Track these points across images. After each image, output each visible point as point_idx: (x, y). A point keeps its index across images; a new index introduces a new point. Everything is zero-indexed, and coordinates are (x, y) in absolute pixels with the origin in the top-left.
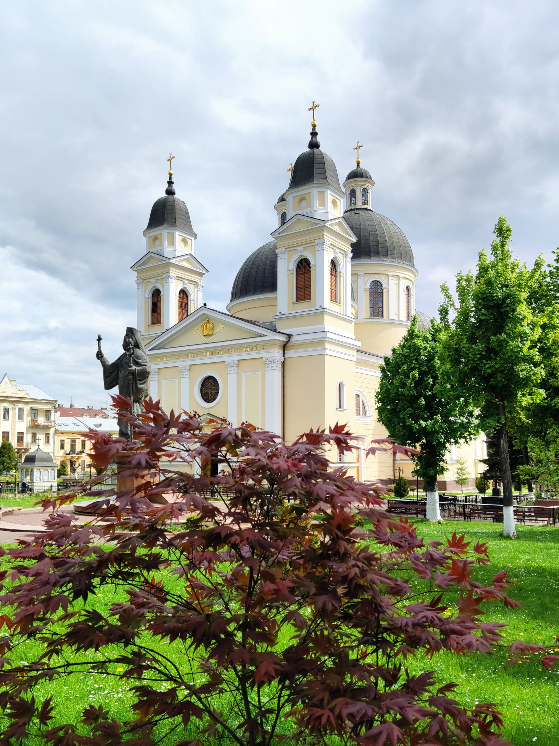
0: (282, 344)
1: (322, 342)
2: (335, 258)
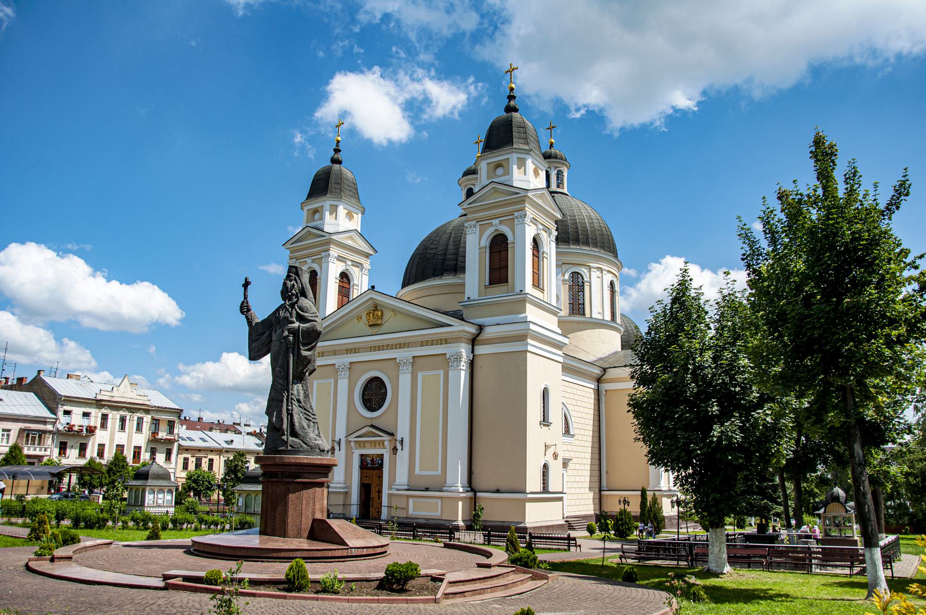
0: (471, 337)
1: (522, 338)
2: (538, 234)
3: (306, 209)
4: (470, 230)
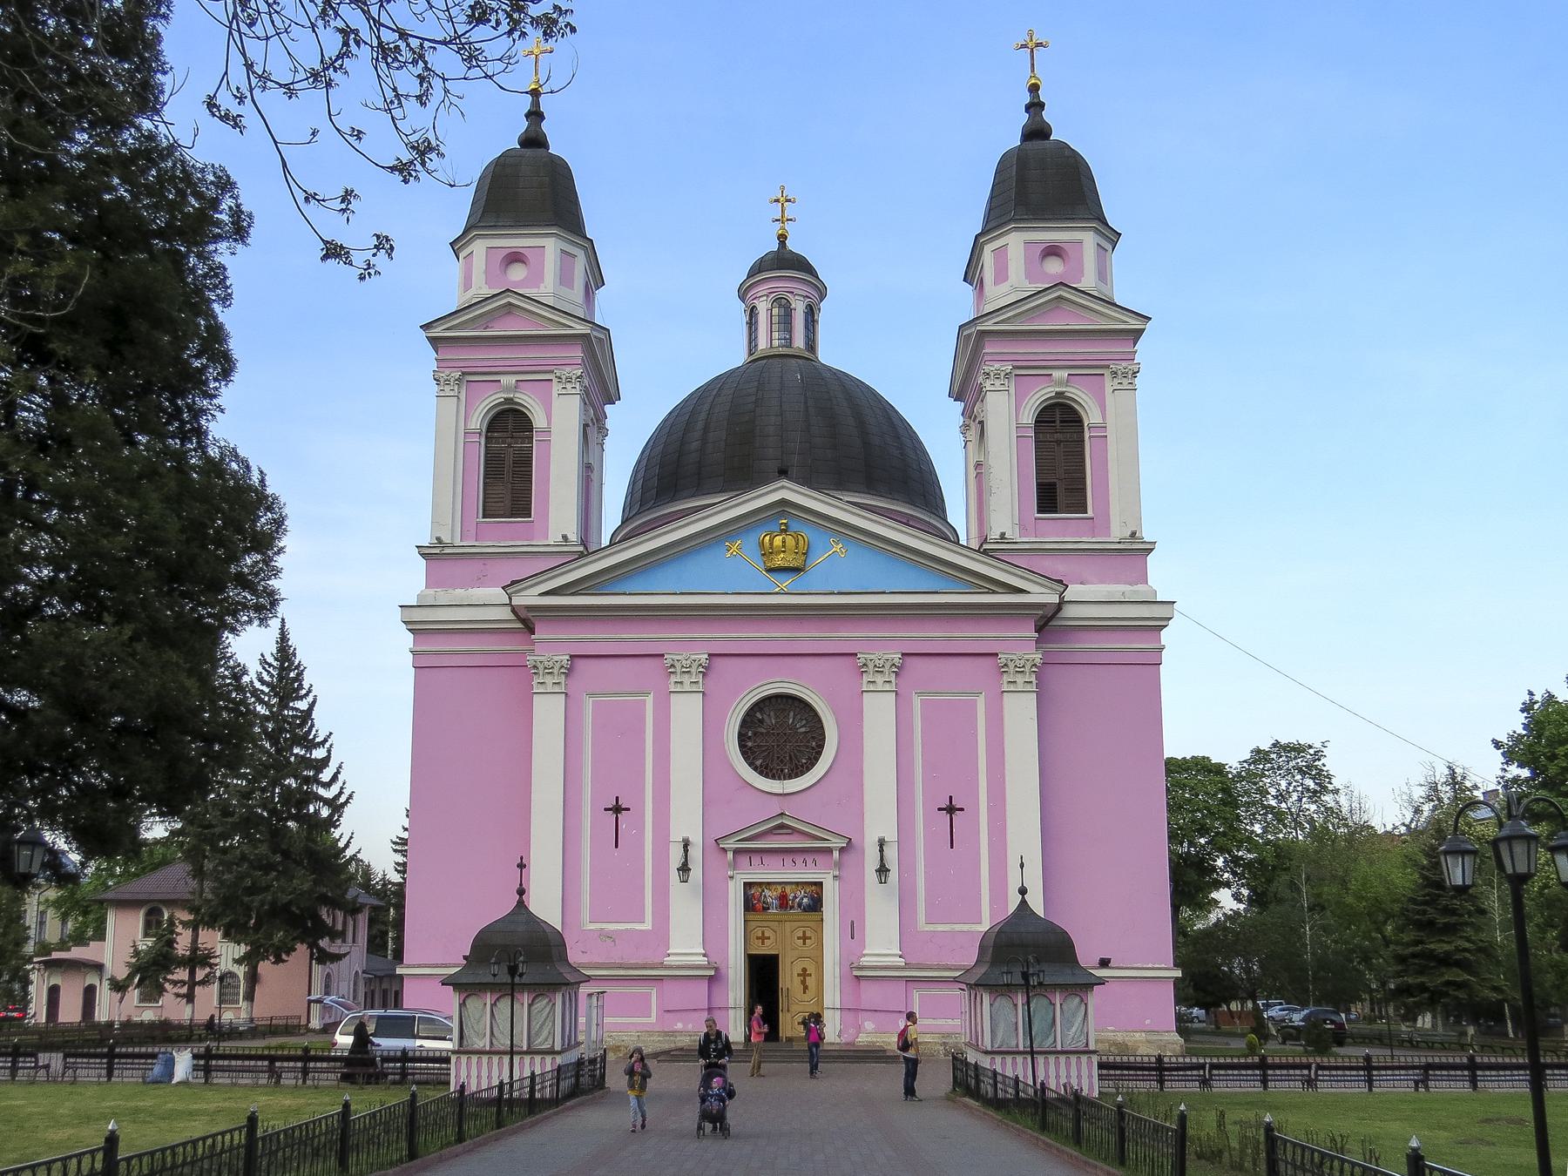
3: (479, 248)
4: (997, 383)
